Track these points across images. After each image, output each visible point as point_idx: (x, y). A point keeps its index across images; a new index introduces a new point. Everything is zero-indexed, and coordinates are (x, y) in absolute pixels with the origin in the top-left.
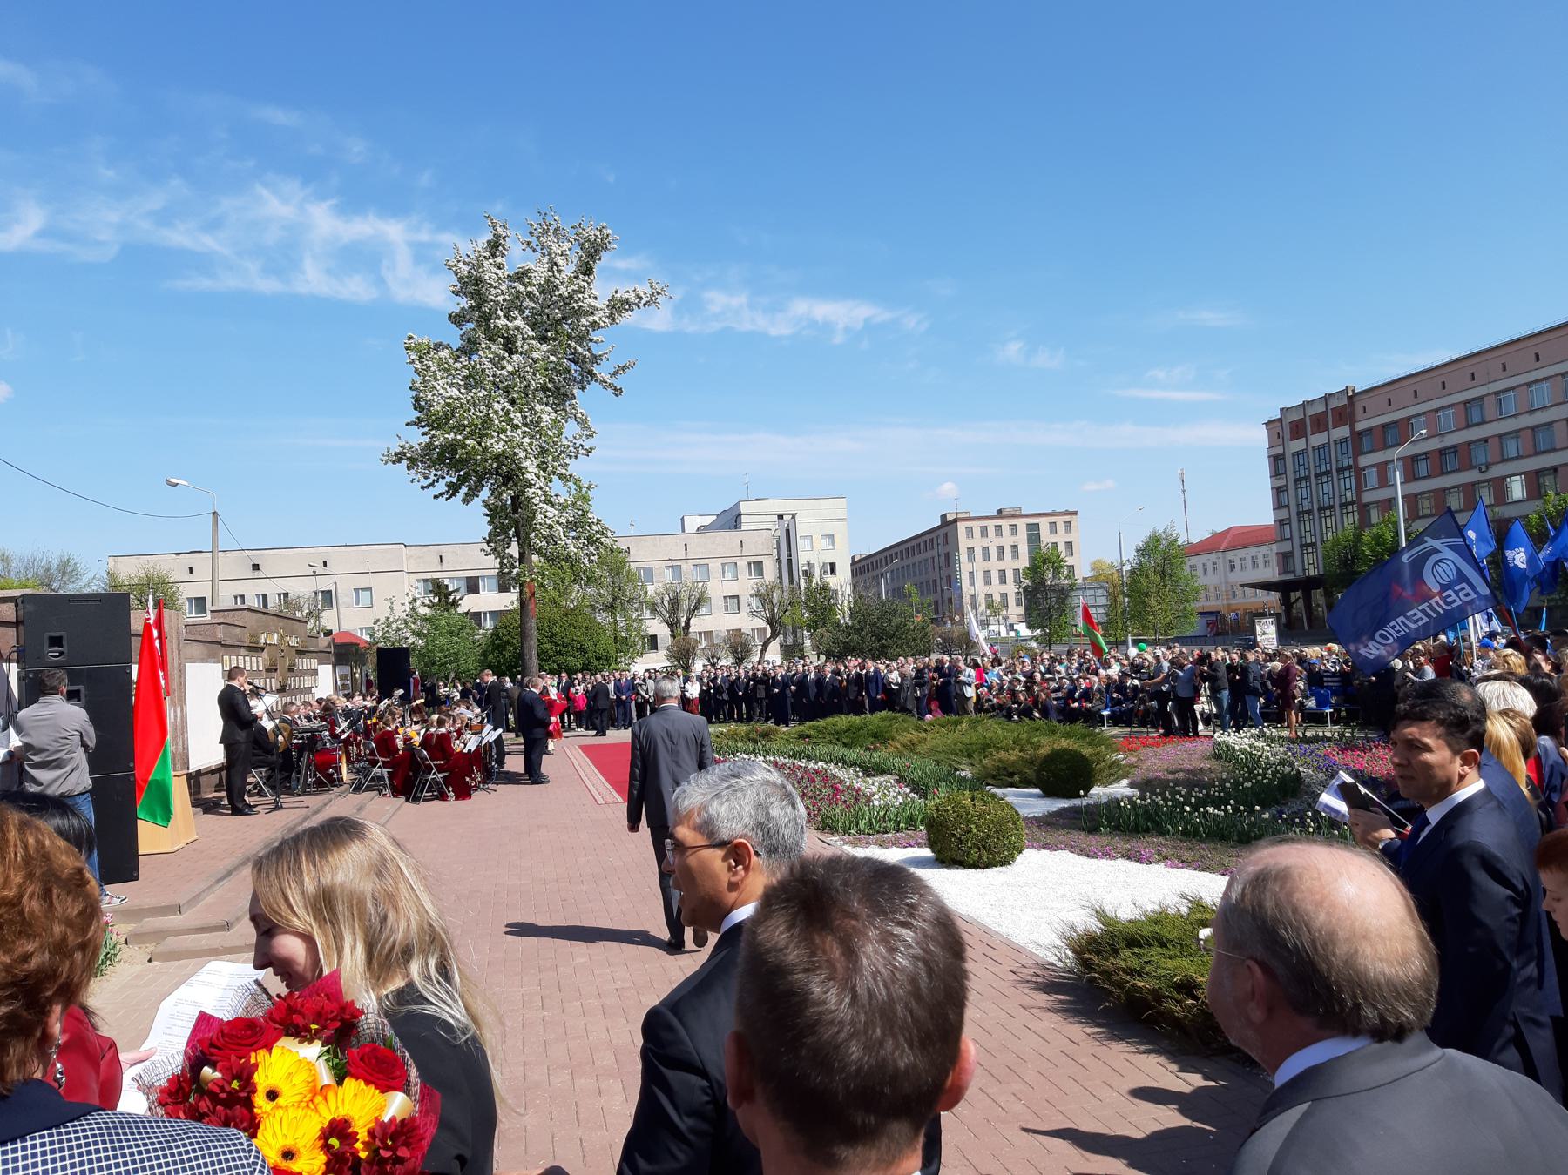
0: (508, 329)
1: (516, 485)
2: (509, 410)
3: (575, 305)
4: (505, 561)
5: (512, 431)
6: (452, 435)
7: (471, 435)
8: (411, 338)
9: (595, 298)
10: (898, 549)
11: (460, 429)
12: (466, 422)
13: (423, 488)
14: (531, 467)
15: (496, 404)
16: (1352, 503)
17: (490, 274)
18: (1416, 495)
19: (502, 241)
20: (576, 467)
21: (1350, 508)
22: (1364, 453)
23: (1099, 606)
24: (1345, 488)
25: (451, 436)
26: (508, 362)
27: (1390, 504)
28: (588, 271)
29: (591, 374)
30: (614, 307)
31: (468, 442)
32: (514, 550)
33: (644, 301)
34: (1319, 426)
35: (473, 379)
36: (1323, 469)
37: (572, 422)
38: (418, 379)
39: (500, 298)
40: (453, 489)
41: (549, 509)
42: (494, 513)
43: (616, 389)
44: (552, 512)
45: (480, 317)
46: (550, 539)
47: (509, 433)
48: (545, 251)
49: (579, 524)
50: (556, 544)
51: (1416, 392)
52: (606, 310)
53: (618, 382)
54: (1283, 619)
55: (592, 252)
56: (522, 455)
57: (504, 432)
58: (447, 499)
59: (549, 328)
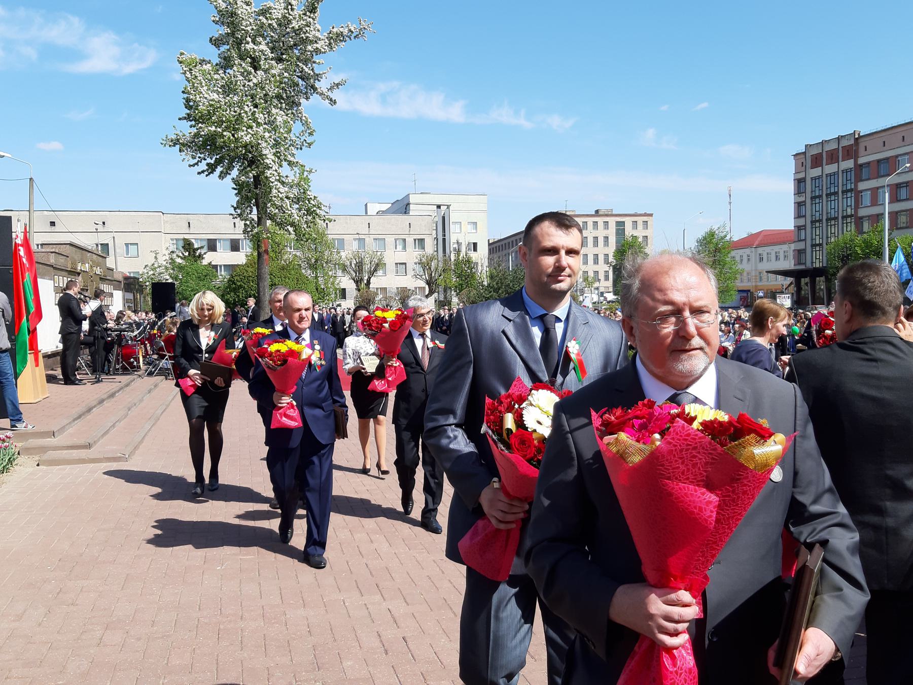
0: (254, 51)
1: (258, 167)
2: (255, 112)
3: (303, 35)
4: (248, 222)
5: (257, 127)
7: (227, 128)
8: (182, 54)
9: (318, 31)
12: (224, 119)
13: (190, 166)
15: (246, 107)
16: (851, 216)
18: (897, 213)
20: (300, 156)
21: (849, 220)
22: (862, 180)
24: (845, 205)
25: (213, 128)
27: (879, 217)
28: (313, 10)
33: (353, 35)
34: (832, 159)
36: (832, 191)
41: (281, 186)
42: (240, 187)
43: (331, 100)
45: (234, 41)
46: (280, 208)
50: (284, 212)
51: (903, 137)
52: (326, 40)
53: (334, 95)
56: (264, 145)
57: (251, 127)
58: (207, 176)
59: (284, 52)
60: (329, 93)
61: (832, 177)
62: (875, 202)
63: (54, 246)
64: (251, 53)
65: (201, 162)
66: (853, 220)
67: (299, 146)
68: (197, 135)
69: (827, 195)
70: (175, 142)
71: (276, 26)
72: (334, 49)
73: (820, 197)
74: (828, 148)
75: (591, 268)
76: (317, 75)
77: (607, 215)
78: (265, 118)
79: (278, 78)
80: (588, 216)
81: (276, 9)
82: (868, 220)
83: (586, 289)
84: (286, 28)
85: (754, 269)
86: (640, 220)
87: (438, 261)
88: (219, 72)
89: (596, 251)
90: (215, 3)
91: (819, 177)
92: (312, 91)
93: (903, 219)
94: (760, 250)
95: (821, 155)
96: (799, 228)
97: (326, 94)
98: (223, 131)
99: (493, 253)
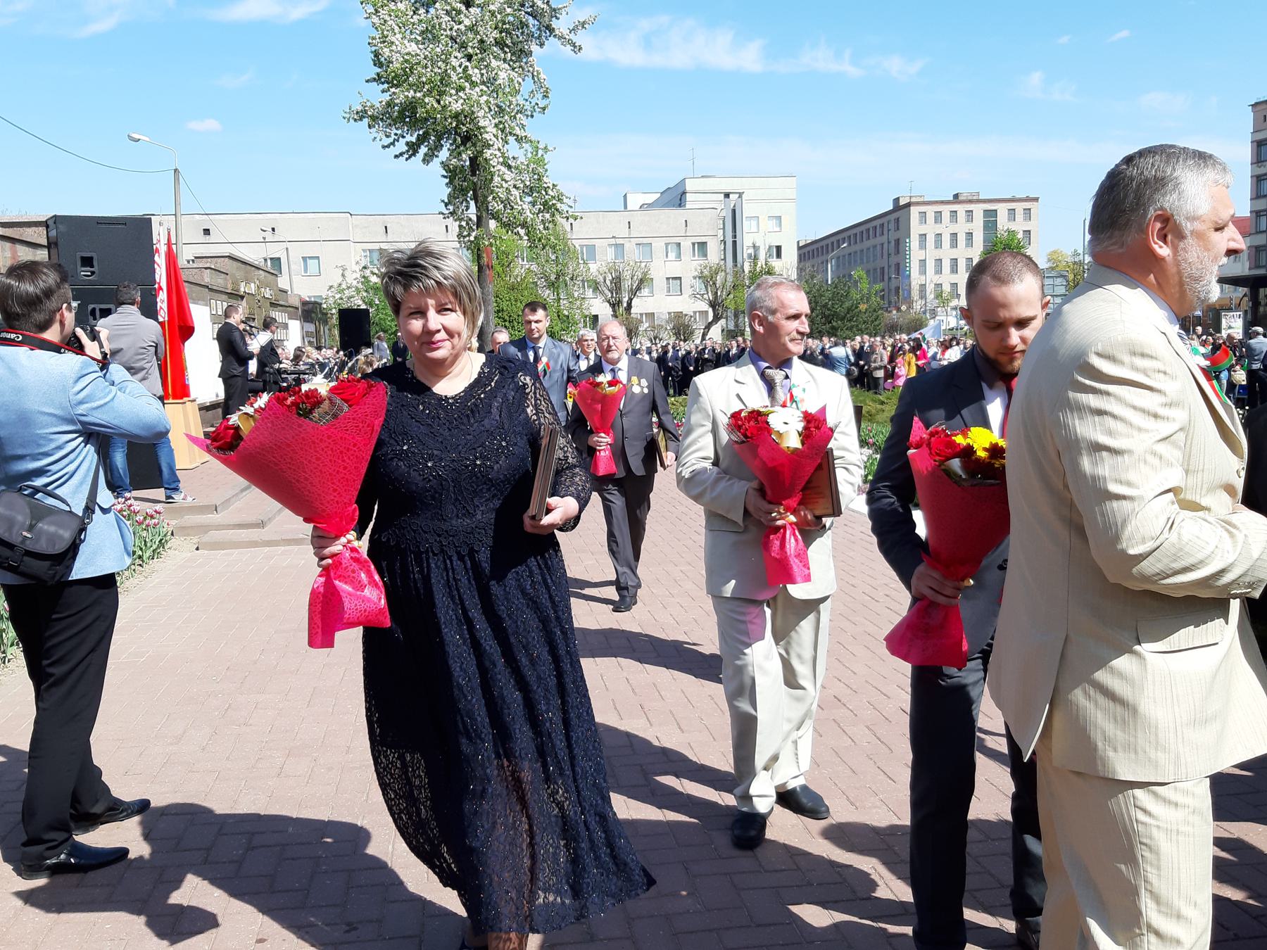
1: (474, 145)
2: (466, 67)
4: (464, 223)
5: (470, 89)
11: (418, 86)
13: (384, 147)
20: (533, 128)
23: (1057, 296)
32: (472, 212)
40: (413, 148)
41: (507, 172)
42: (452, 174)
43: (575, 47)
44: (509, 175)
46: (507, 203)
50: (512, 208)
53: (578, 39)
54: (1249, 316)
56: (481, 114)
57: (461, 89)
58: (407, 159)
60: (572, 36)
65: (398, 141)
67: (529, 113)
70: (361, 115)
76: (555, 10)
77: (970, 202)
78: (482, 75)
79: (499, 16)
80: (942, 202)
83: (939, 309)
86: (1019, 207)
87: (726, 274)
88: (420, 12)
89: (954, 253)
92: (548, 34)
97: (567, 37)
98: (424, 96)
99: (805, 260)
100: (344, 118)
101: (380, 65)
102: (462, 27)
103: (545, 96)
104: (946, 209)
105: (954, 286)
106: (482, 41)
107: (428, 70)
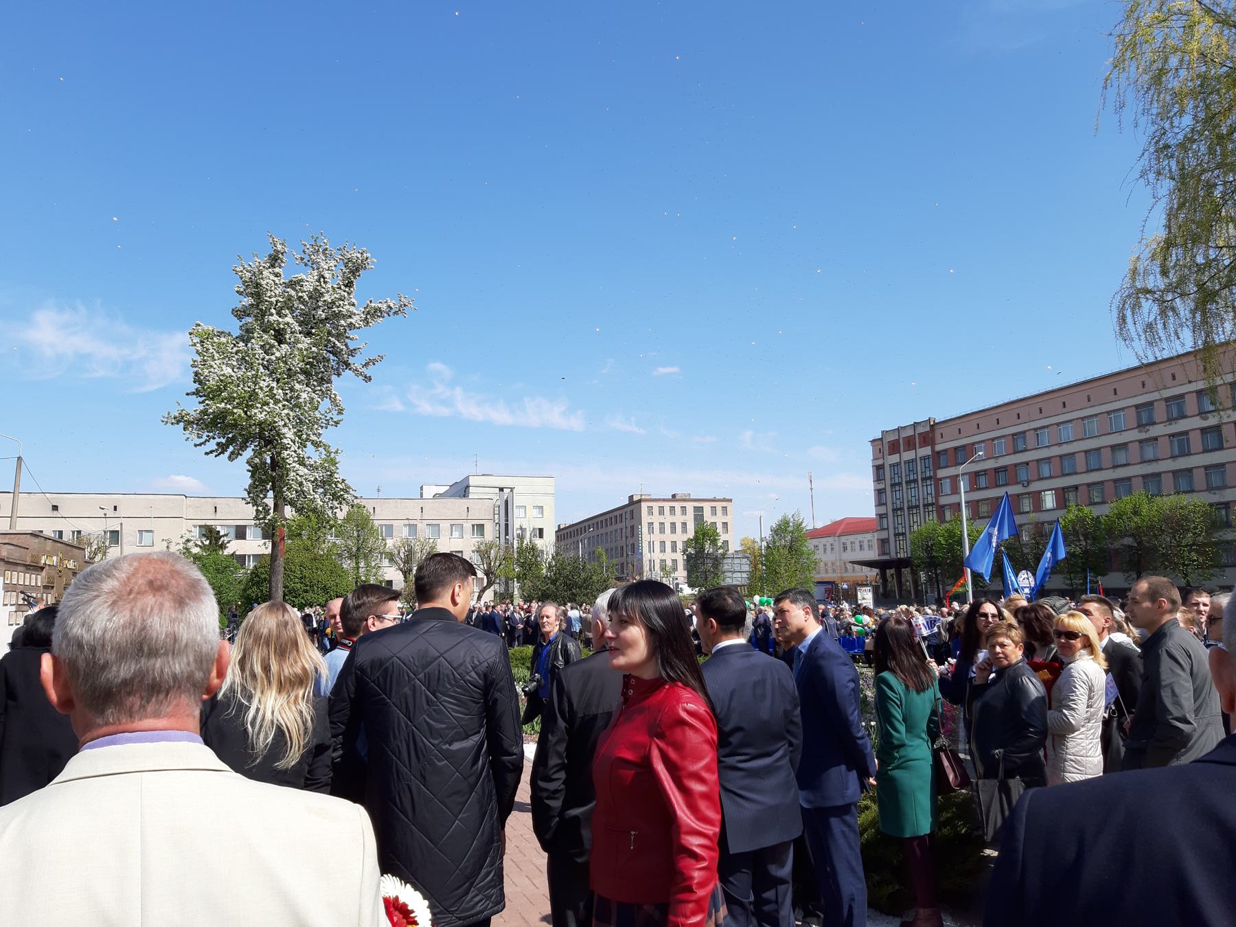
0: (279, 323)
1: (274, 448)
2: (273, 388)
3: (336, 309)
4: (260, 508)
6: (223, 405)
9: (353, 305)
10: (591, 522)
11: (230, 400)
13: (196, 445)
14: (289, 434)
17: (267, 279)
19: (280, 256)
20: (328, 436)
26: (277, 349)
28: (349, 285)
29: (347, 365)
30: (368, 313)
31: (235, 411)
32: (270, 501)
33: (393, 311)
35: (245, 361)
37: (327, 401)
38: (199, 359)
39: (273, 300)
42: (255, 470)
43: (366, 377)
44: (303, 471)
46: (301, 493)
47: (271, 405)
48: (314, 266)
49: (328, 484)
50: (306, 498)
52: (362, 315)
53: (367, 371)
55: (354, 269)
57: (268, 404)
58: (216, 456)
60: (364, 370)
61: (896, 468)
62: (955, 490)
63: (13, 536)
64: (275, 325)
66: (934, 509)
68: (204, 412)
69: (907, 482)
71: (307, 299)
72: (371, 324)
73: (900, 484)
74: (904, 434)
75: (669, 556)
76: (351, 351)
77: (684, 500)
80: (664, 500)
81: (308, 281)
82: (950, 508)
84: (318, 301)
85: (838, 558)
86: (719, 505)
89: (674, 537)
90: (240, 274)
91: (898, 464)
92: (345, 367)
93: (984, 509)
94: (843, 539)
95: (898, 441)
96: (881, 516)
97: (360, 370)
100: (163, 421)
101: (200, 383)
102: (273, 358)
103: (340, 413)
104: (667, 505)
105: (675, 561)
106: (290, 370)
107: (239, 388)
